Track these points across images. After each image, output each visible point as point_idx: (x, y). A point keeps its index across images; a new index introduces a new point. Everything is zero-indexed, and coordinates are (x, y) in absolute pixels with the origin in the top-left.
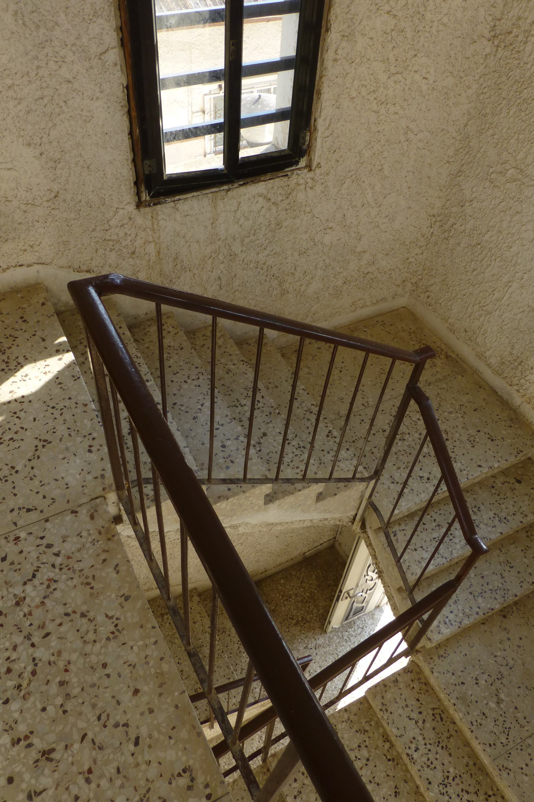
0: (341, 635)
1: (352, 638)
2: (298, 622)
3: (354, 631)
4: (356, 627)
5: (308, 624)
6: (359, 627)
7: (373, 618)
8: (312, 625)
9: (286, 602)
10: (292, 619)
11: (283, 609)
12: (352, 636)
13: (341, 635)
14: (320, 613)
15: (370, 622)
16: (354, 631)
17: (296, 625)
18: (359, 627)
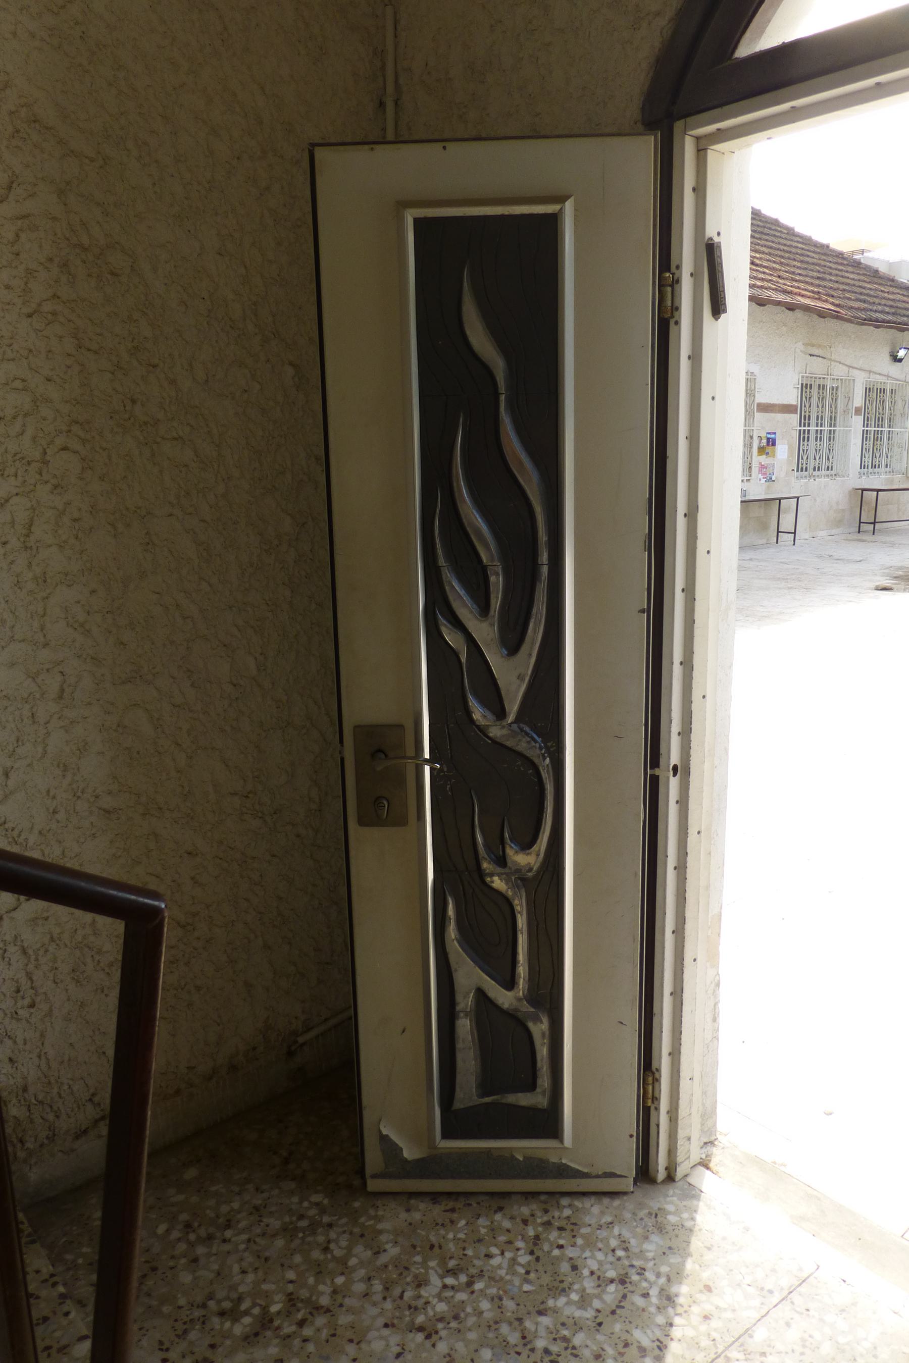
0: (514, 1338)
1: (578, 1340)
2: (266, 1321)
3: (584, 1301)
4: (589, 1285)
5: (320, 1321)
6: (602, 1282)
7: (660, 1229)
8: (344, 1319)
9: (200, 1250)
10: (232, 1314)
11: (186, 1278)
12: (577, 1326)
13: (514, 1338)
14: (383, 1259)
15: (651, 1248)
16: (584, 1301)
17: (252, 1338)
18: (602, 1282)
